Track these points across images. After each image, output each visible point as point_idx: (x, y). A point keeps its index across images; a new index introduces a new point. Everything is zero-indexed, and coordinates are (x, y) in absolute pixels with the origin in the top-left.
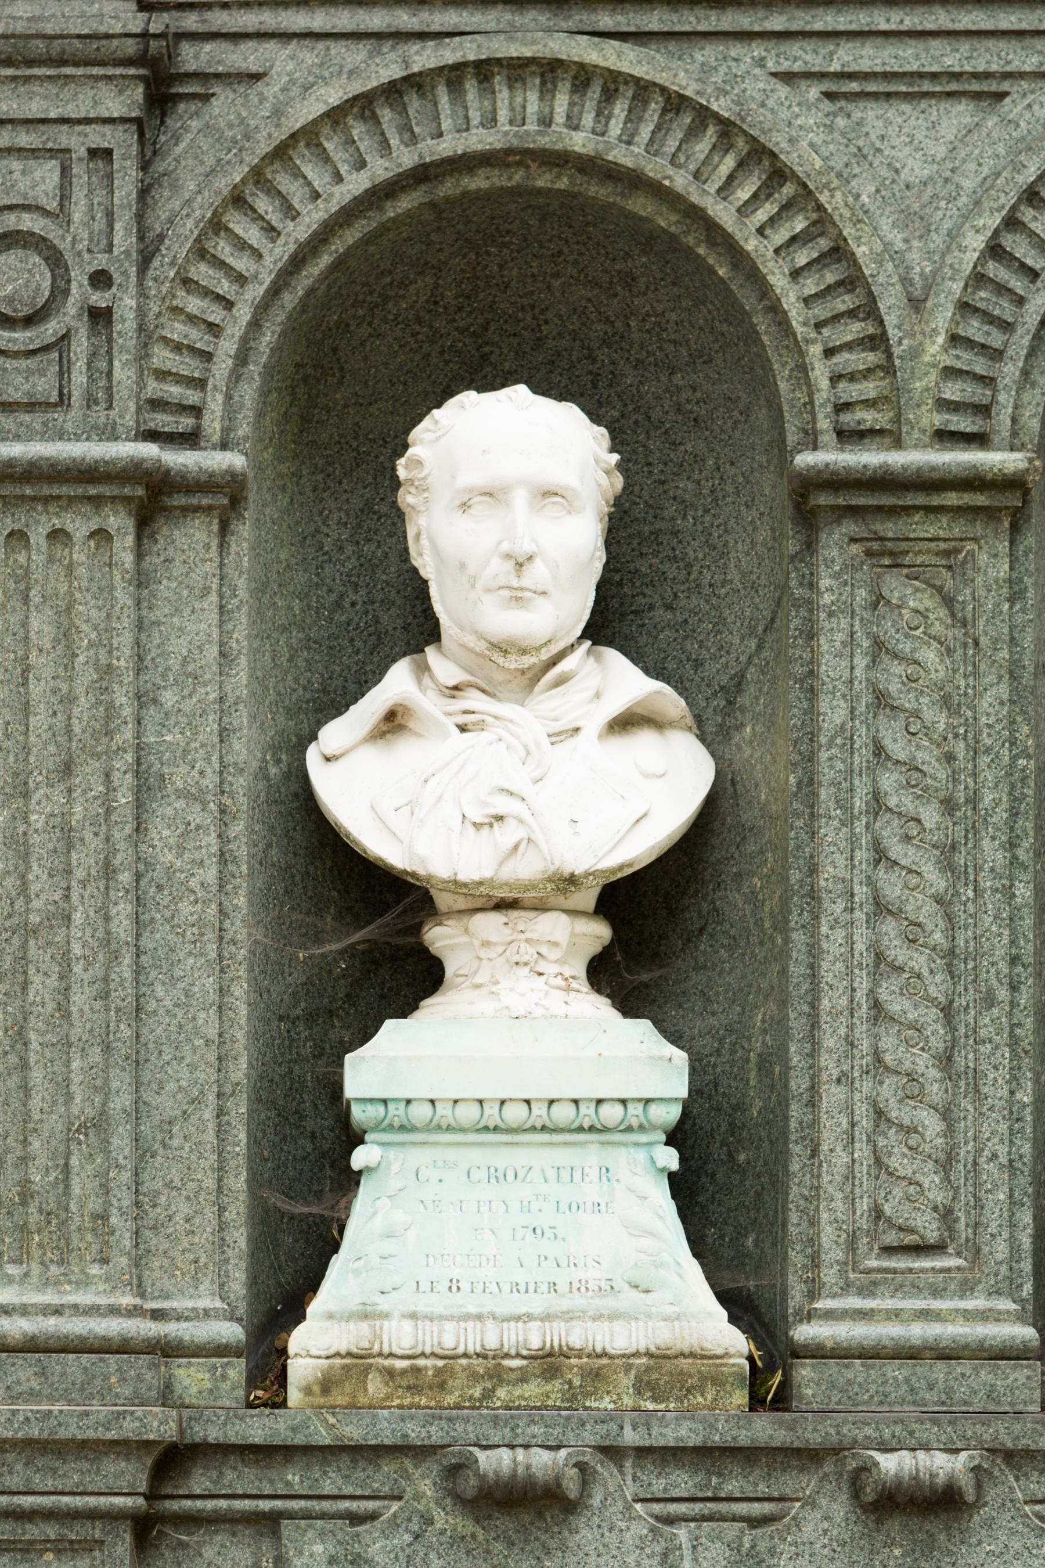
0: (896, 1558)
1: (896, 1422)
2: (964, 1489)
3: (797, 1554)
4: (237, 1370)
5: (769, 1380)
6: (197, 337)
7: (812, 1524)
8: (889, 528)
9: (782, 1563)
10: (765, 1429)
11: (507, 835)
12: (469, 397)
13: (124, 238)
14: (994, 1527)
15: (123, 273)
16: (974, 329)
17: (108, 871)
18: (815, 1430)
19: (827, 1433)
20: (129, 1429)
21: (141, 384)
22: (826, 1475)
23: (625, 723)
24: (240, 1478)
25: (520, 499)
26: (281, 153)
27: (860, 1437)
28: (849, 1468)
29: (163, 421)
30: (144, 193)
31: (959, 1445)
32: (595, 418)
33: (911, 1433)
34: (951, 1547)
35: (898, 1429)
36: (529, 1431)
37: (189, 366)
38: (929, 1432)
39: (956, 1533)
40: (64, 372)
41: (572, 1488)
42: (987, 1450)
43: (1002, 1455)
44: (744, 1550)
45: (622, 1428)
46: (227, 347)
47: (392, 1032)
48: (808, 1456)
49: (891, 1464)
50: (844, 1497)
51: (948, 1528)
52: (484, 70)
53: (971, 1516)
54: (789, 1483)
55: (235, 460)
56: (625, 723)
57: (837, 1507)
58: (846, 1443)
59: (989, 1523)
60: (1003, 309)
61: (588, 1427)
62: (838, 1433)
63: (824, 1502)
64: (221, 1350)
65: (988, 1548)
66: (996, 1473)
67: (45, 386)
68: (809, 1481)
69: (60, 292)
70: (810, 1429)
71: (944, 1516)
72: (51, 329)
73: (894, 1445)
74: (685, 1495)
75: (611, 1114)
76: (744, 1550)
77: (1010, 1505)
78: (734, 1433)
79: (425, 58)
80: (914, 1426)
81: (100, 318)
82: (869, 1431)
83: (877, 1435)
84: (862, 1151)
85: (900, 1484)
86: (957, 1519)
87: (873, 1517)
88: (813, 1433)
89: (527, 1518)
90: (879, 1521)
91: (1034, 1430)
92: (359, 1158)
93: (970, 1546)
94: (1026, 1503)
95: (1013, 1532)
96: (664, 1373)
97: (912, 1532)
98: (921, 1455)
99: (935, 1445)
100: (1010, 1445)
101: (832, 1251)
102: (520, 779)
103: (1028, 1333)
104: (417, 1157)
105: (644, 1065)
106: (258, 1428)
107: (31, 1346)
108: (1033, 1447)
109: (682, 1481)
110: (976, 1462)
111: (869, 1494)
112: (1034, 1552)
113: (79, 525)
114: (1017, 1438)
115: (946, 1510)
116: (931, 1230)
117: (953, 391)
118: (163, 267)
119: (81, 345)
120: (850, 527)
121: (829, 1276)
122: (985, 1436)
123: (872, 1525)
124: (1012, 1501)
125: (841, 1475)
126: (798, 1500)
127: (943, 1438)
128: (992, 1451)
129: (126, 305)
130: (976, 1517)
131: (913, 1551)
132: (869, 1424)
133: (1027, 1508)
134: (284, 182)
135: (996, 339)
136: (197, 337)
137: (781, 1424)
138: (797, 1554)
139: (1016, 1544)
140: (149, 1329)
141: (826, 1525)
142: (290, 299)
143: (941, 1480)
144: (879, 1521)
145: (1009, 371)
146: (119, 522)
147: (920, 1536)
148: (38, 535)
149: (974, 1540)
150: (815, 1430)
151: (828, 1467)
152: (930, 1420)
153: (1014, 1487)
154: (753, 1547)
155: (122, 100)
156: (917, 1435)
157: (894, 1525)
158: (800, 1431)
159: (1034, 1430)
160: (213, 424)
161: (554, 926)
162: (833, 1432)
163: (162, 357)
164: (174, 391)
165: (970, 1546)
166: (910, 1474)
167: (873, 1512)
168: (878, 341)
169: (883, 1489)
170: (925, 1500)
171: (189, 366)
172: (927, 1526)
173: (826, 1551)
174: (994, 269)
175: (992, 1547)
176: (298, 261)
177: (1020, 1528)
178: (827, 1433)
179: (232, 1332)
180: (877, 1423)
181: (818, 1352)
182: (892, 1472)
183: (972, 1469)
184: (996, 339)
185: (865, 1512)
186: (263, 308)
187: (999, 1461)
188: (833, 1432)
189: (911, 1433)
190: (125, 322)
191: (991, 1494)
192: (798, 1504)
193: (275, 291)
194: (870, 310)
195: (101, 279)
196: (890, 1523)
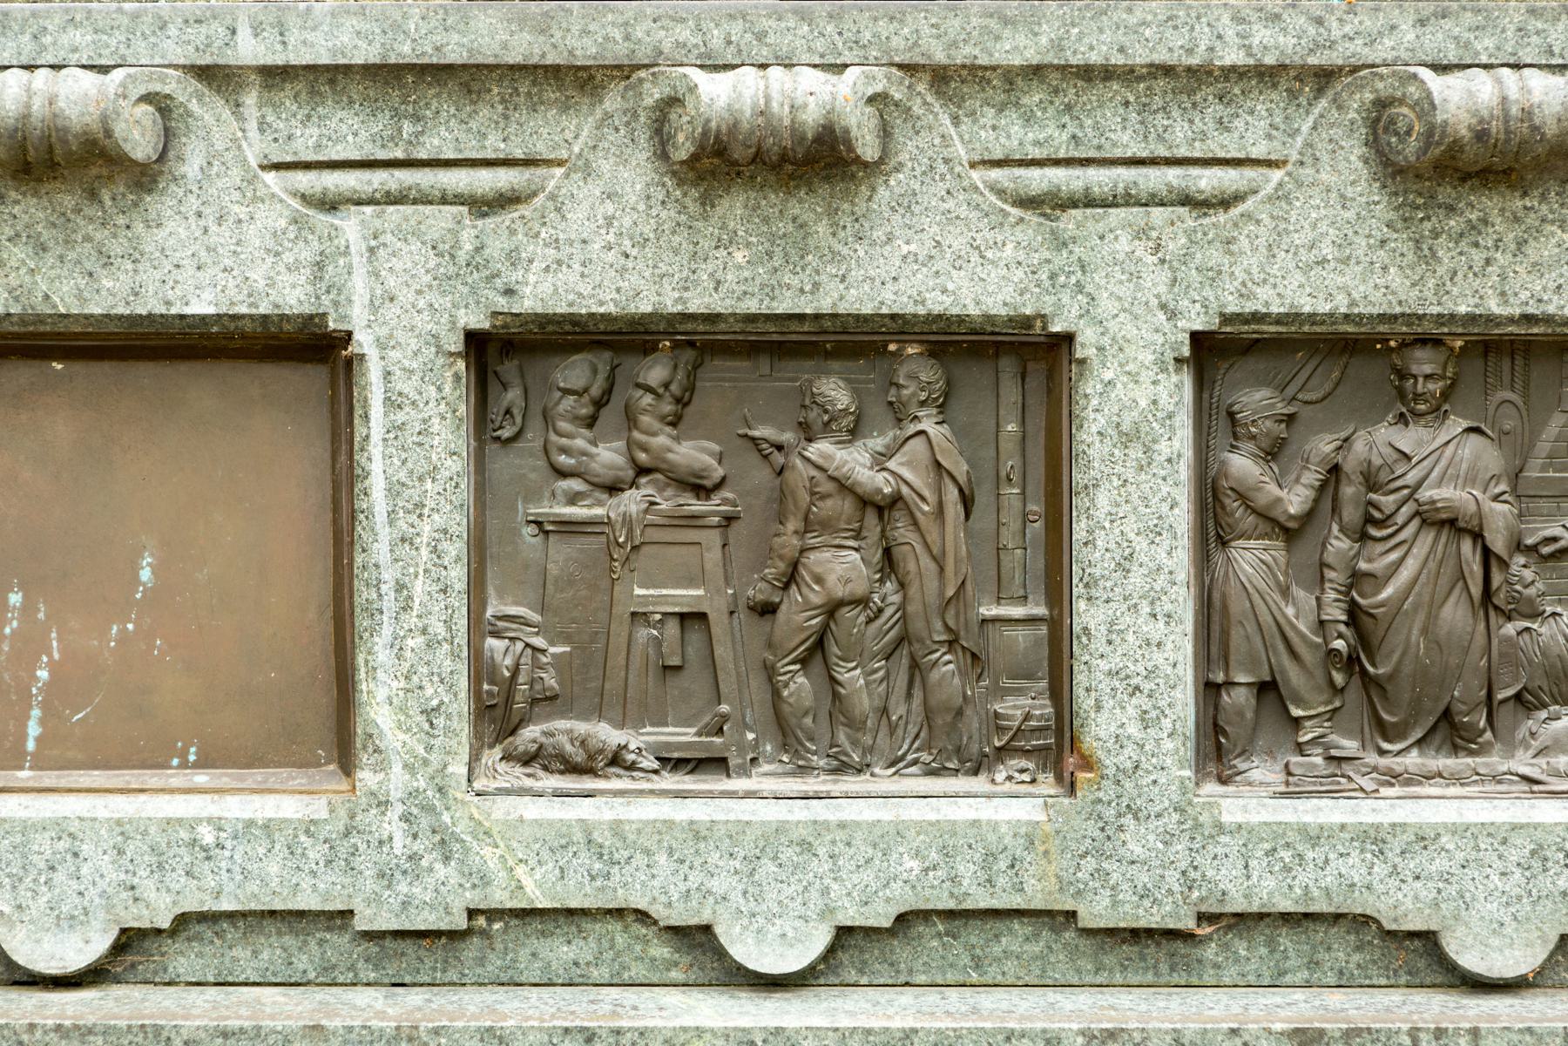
0: (740, 267)
1: (731, 17)
2: (854, 132)
3: (559, 263)
7: (586, 205)
9: (532, 278)
14: (916, 209)
18: (585, 32)
19: (606, 38)
22: (608, 116)
27: (667, 46)
28: (649, 101)
31: (847, 57)
33: (760, 36)
34: (838, 247)
35: (736, 29)
36: (65, 40)
38: (791, 34)
39: (847, 220)
41: (139, 140)
42: (900, 66)
43: (927, 77)
44: (462, 256)
45: (234, 32)
48: (576, 81)
49: (721, 95)
50: (642, 155)
51: (832, 212)
53: (874, 190)
54: (545, 130)
58: (642, 57)
59: (905, 204)
61: (172, 31)
62: (627, 38)
63: (605, 165)
65: (905, 249)
66: (917, 110)
68: (579, 127)
70: (575, 29)
71: (824, 190)
73: (730, 60)
74: (355, 155)
76: (462, 256)
77: (942, 168)
78: (438, 39)
80: (766, 23)
82: (684, 33)
83: (698, 40)
85: (736, 124)
86: (848, 195)
87: (694, 193)
89: (68, 201)
90: (706, 201)
91: (985, 29)
93: (873, 244)
94: (973, 165)
95: (951, 219)
97: (766, 220)
98: (775, 72)
99: (805, 58)
100: (940, 57)
108: (983, 60)
109: (349, 130)
110: (879, 88)
111: (683, 150)
112: (989, 254)
114: (954, 44)
115: (827, 179)
122: (896, 42)
123: (693, 208)
124: (946, 161)
125: (635, 115)
126: (560, 163)
127: (820, 45)
128: (908, 68)
130: (882, 192)
131: (770, 254)
132: (683, 20)
133: (976, 175)
137: (522, 21)
138: (559, 263)
139: (957, 241)
141: (610, 208)
143: (812, 117)
144: (706, 201)
147: (783, 227)
149: (879, 234)
150: (585, 32)
151: (612, 101)
152: (795, 12)
153: (946, 134)
154: (478, 250)
156: (770, 39)
157: (734, 206)
158: (558, 34)
159: (985, 29)
162: (617, 34)
165: (873, 244)
166: (755, 105)
167: (695, 184)
169: (705, 134)
170: (784, 158)
172: (795, 209)
173: (611, 256)
175: (913, 247)
177: (963, 211)
178: (606, 38)
180: (698, 18)
182: (722, 102)
183: (871, 100)
185: (681, 183)
187: (921, 87)
188: (617, 34)
189: (760, 36)
191: (908, 148)
192: (559, 171)
196: (726, 202)
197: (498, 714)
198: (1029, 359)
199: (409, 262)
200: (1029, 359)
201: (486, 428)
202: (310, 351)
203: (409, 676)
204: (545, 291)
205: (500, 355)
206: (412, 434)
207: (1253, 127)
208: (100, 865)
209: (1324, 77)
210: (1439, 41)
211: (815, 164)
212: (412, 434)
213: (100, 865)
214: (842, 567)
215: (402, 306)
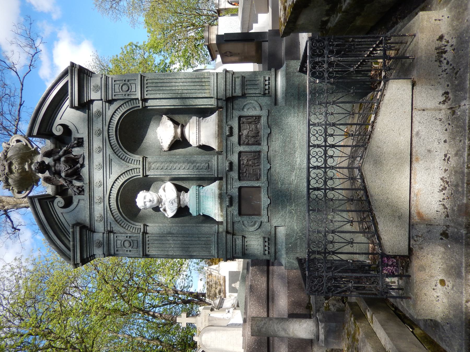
4: (220, 226)
5: (221, 179)
6: (132, 228)
8: (147, 169)
10: (224, 179)
11: (173, 202)
12: (137, 204)
13: (123, 235)
15: (126, 235)
16: (130, 161)
17: (177, 237)
20: (225, 236)
21: (136, 234)
23: (164, 190)
24: (229, 226)
25: (145, 201)
26: (116, 221)
29: (139, 231)
30: (121, 233)
32: (139, 193)
37: (134, 229)
40: (134, 240)
41: (230, 197)
46: (133, 226)
47: (191, 211)
52: (109, 203)
55: (142, 225)
56: (164, 190)
57: (231, 173)
60: (129, 159)
64: (218, 227)
67: (136, 242)
69: (128, 240)
72: (131, 241)
75: (197, 192)
79: (108, 209)
81: (130, 237)
84: (200, 171)
88: (225, 175)
92: (201, 214)
96: (220, 188)
101: (209, 173)
102: (169, 200)
103: (216, 156)
104: (201, 209)
105: (193, 189)
106: (225, 224)
107: (218, 244)
113: (147, 239)
116: (207, 165)
117: (135, 163)
118: (126, 231)
119: (132, 239)
120: (147, 172)
121: (211, 174)
129: (129, 235)
134: (119, 221)
135: (131, 160)
136: (132, 228)
140: (216, 234)
142: (129, 220)
145: (134, 159)
146: (147, 236)
148: (148, 243)
155: (112, 235)
160: (139, 227)
161: (181, 197)
163: (134, 231)
164: (136, 230)
168: (131, 170)
171: (134, 229)
174: (125, 160)
176: (125, 219)
179: (217, 226)
181: (218, 175)
184: (131, 160)
186: (130, 223)
190: (131, 235)
193: (128, 222)
194: (129, 171)
195: (127, 237)
197: (258, 179)
198: (240, 153)
199: (235, 184)
200: (240, 153)
201: (244, 180)
202: (240, 188)
203: (256, 184)
204: (237, 177)
205: (240, 179)
206: (245, 184)
207: (229, 143)
208: (265, 199)
209: (226, 139)
210: (225, 134)
211: (231, 164)
212: (245, 184)
213: (265, 199)
214: (250, 163)
215: (238, 184)
